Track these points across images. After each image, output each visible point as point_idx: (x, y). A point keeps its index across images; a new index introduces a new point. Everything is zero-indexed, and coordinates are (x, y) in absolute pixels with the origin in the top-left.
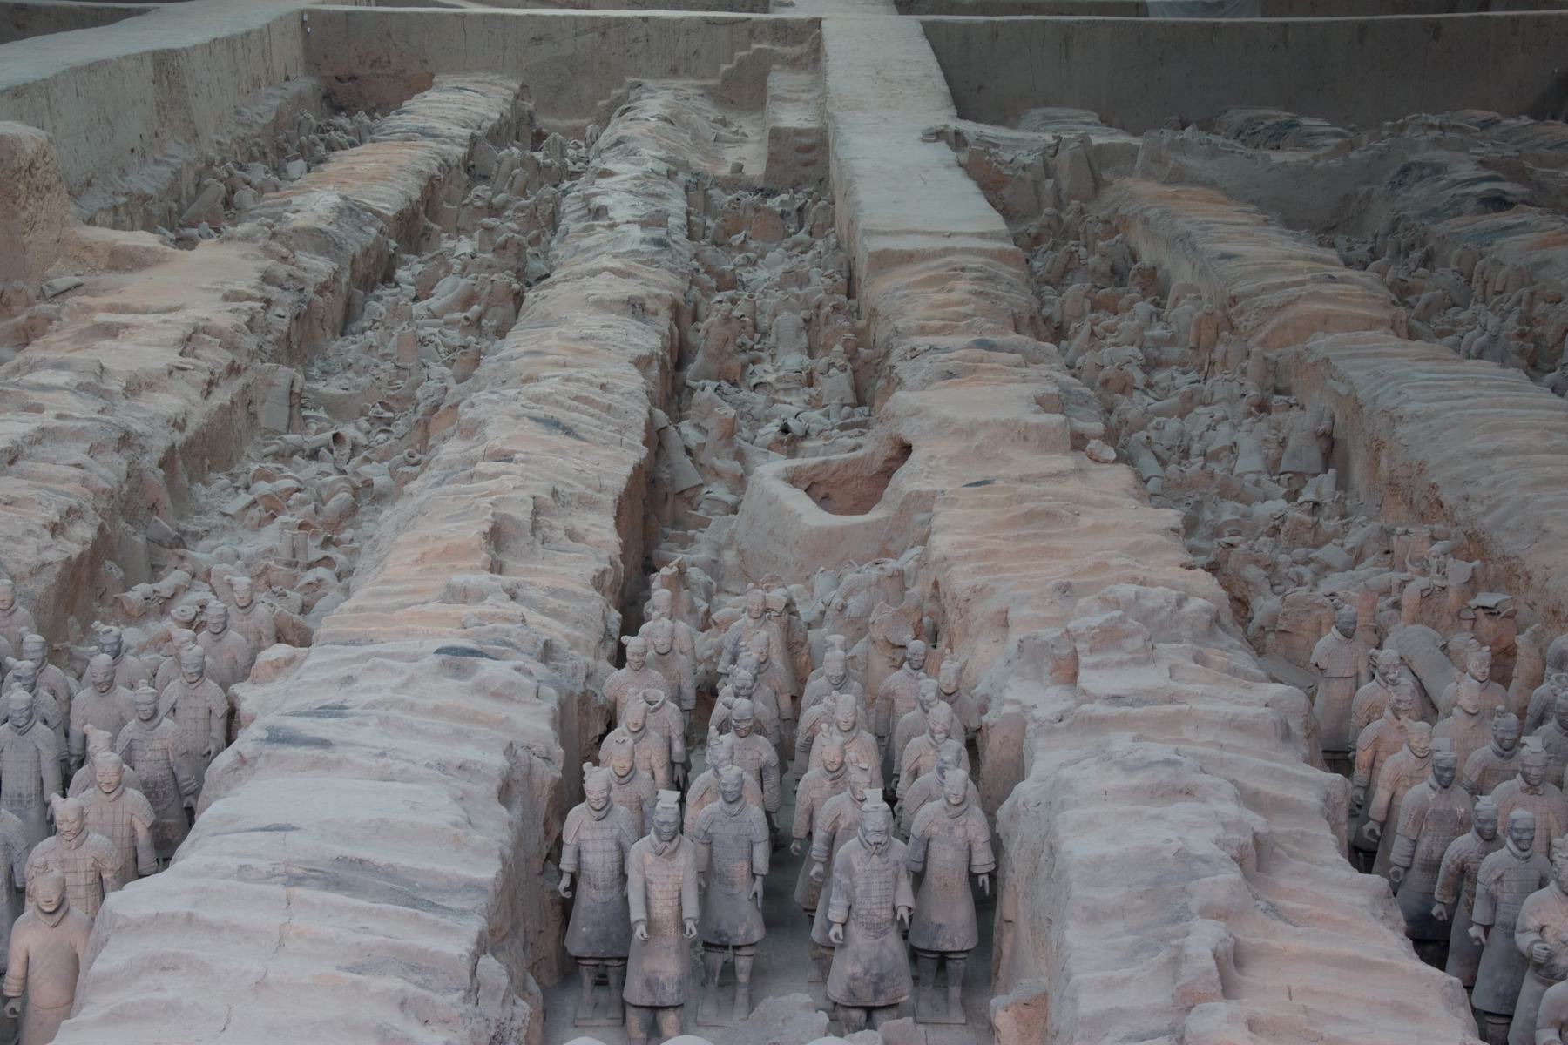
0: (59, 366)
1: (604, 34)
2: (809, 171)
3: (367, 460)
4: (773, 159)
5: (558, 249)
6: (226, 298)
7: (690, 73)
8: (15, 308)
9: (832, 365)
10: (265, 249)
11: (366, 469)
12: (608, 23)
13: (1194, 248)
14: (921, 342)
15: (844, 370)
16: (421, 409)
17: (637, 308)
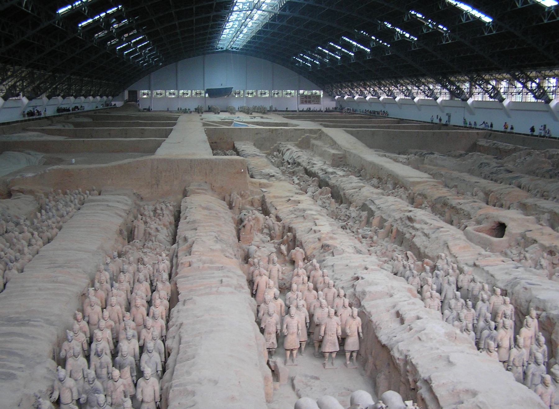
0: (311, 210)
1: (272, 132)
2: (341, 163)
3: (358, 229)
4: (333, 160)
5: (333, 181)
6: (297, 193)
7: (292, 141)
8: (246, 197)
9: (426, 206)
10: (289, 182)
11: (359, 231)
12: (273, 130)
13: (464, 180)
14: (461, 201)
15: (428, 207)
16: (363, 218)
17: (383, 194)
